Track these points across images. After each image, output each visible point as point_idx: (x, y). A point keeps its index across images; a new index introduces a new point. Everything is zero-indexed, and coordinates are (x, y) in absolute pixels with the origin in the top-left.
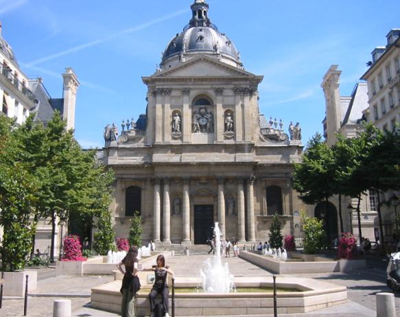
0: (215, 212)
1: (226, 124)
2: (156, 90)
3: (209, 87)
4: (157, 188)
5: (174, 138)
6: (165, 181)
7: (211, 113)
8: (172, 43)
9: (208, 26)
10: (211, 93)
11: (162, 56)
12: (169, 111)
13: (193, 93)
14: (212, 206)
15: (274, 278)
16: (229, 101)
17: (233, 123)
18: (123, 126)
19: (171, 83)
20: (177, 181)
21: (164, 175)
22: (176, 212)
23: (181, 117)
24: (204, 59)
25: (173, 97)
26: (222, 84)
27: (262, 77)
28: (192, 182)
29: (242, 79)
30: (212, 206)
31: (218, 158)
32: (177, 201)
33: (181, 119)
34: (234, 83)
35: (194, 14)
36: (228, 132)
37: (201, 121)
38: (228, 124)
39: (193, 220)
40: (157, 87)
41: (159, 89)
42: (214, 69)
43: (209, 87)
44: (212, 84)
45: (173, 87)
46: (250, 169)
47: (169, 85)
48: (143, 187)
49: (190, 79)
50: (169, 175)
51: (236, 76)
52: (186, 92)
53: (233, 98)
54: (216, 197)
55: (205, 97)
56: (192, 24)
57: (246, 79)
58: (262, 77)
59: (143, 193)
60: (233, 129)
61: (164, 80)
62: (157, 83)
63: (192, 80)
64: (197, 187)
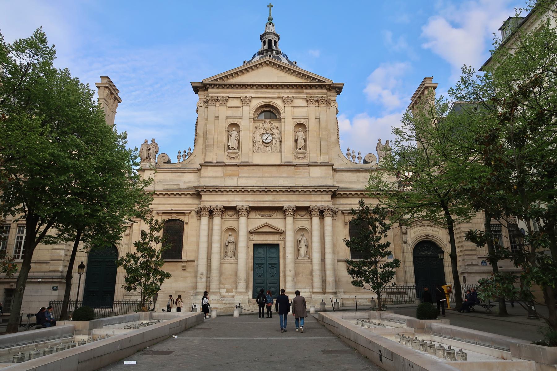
0: (281, 254)
1: (296, 141)
2: (208, 98)
4: (205, 220)
5: (231, 158)
7: (277, 128)
10: (278, 103)
12: (225, 124)
13: (256, 103)
14: (278, 245)
16: (301, 113)
17: (305, 140)
18: (179, 157)
19: (228, 90)
21: (214, 204)
22: (229, 254)
25: (230, 107)
26: (291, 93)
28: (253, 215)
29: (315, 86)
30: (276, 246)
31: (285, 182)
32: (232, 239)
34: (305, 91)
36: (300, 151)
37: (265, 137)
38: (299, 142)
39: (251, 264)
40: (210, 95)
41: (212, 97)
43: (276, 96)
44: (279, 93)
45: (230, 95)
46: (328, 197)
47: (226, 93)
48: (186, 221)
50: (220, 204)
51: (308, 82)
52: (246, 101)
54: (282, 233)
59: (185, 226)
60: (305, 147)
64: (257, 221)
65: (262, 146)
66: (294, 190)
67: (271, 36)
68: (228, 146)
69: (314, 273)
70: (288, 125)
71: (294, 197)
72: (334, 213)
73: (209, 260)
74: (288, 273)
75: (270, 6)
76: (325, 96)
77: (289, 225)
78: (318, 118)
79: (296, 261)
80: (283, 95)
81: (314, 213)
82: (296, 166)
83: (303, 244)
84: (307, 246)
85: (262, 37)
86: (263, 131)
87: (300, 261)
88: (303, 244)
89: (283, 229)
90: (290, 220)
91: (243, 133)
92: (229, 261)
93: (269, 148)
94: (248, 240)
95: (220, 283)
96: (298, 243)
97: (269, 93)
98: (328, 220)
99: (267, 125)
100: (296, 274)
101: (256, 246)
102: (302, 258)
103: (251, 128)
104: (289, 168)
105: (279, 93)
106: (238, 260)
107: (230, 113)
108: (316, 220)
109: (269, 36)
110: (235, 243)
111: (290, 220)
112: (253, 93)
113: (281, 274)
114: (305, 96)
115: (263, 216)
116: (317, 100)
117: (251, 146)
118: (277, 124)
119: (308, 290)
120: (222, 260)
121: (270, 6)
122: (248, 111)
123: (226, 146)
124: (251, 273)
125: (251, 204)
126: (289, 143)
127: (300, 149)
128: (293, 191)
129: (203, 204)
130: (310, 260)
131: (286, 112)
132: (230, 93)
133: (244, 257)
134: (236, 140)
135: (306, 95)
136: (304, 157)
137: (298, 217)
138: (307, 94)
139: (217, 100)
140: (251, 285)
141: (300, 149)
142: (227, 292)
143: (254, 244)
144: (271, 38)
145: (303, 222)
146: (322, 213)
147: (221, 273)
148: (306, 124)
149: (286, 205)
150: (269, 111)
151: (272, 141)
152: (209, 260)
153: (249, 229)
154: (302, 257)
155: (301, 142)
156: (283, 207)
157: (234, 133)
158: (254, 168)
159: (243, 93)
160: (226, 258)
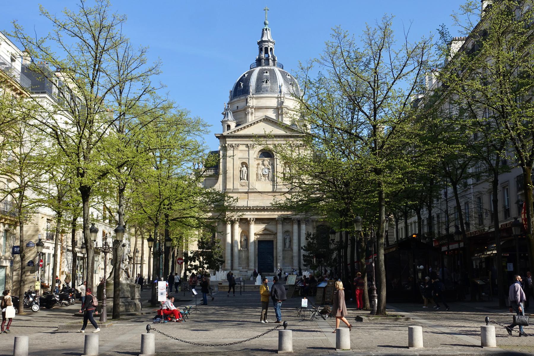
0: (275, 247)
8: (238, 84)
9: (274, 65)
11: (229, 94)
12: (238, 163)
20: (243, 222)
26: (281, 140)
30: (272, 242)
33: (247, 167)
35: (261, 50)
39: (257, 253)
54: (275, 234)
56: (259, 62)
72: (307, 221)
74: (278, 258)
79: (283, 250)
83: (288, 240)
85: (259, 43)
87: (286, 250)
88: (288, 240)
90: (280, 227)
91: (250, 169)
95: (239, 264)
96: (284, 240)
98: (303, 227)
100: (284, 258)
108: (296, 227)
113: (275, 259)
119: (290, 268)
124: (257, 258)
125: (256, 217)
137: (285, 224)
140: (257, 265)
144: (267, 46)
145: (288, 227)
146: (299, 222)
147: (239, 258)
157: (245, 169)
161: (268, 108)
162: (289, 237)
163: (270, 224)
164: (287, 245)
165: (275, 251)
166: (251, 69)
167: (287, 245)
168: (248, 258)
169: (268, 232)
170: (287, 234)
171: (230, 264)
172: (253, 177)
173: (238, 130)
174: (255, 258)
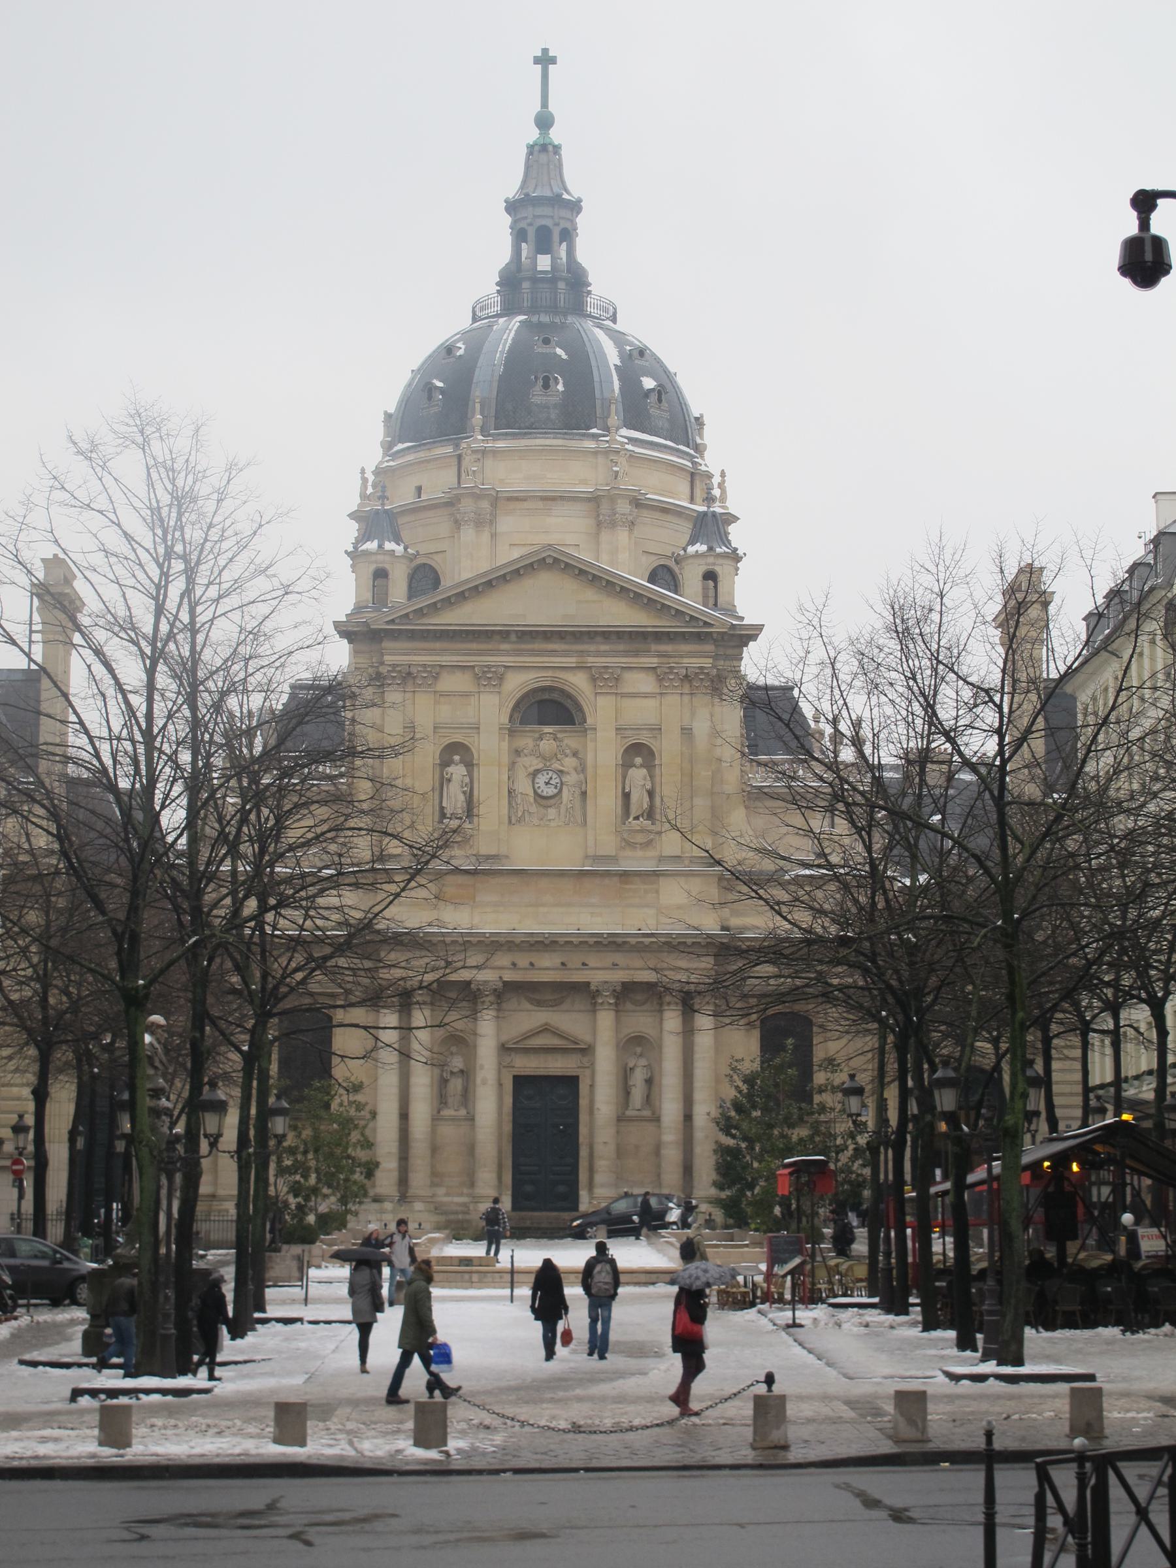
0: (583, 1102)
1: (626, 796)
2: (384, 670)
3: (571, 661)
6: (419, 996)
7: (575, 754)
10: (579, 683)
13: (517, 684)
15: (794, 1318)
16: (641, 712)
17: (651, 794)
19: (438, 645)
22: (450, 1100)
23: (469, 765)
24: (556, 560)
25: (443, 694)
26: (616, 654)
27: (760, 628)
30: (572, 1082)
32: (457, 1063)
34: (654, 647)
35: (519, 236)
37: (541, 779)
38: (634, 798)
39: (508, 1128)
42: (590, 594)
43: (571, 661)
45: (446, 659)
49: (504, 634)
52: (490, 678)
53: (651, 703)
54: (587, 1051)
55: (555, 696)
57: (699, 637)
58: (760, 628)
61: (412, 635)
62: (387, 644)
63: (513, 637)
64: (527, 1018)
65: (533, 809)
66: (619, 940)
67: (547, 211)
68: (442, 808)
69: (663, 1152)
70: (603, 750)
71: (619, 958)
73: (404, 1116)
74: (599, 1149)
75: (545, 60)
76: (707, 663)
77: (604, 1031)
78: (687, 732)
79: (621, 1119)
80: (590, 659)
81: (668, 999)
82: (625, 875)
83: (638, 1077)
84: (649, 1082)
86: (537, 764)
87: (631, 1120)
89: (588, 1038)
90: (605, 1019)
92: (453, 1119)
93: (552, 812)
94: (501, 1067)
95: (434, 1174)
96: (625, 1074)
97: (553, 653)
98: (704, 1022)
99: (547, 745)
100: (620, 1152)
101: (521, 1083)
102: (637, 1113)
103: (505, 759)
104: (607, 881)
105: (582, 653)
106: (477, 1118)
107: (445, 712)
108: (672, 1020)
109: (539, 211)
110: (467, 1074)
111: (605, 1019)
112: (507, 653)
113: (583, 1153)
114: (653, 661)
115: (539, 1003)
116: (686, 676)
117: (505, 811)
118: (571, 741)
120: (436, 1119)
121: (545, 60)
122: (491, 710)
123: (437, 814)
125: (509, 976)
126: (606, 801)
127: (637, 818)
128: (614, 942)
129: (384, 974)
130: (656, 1119)
131: (601, 711)
132: (443, 652)
133: (490, 1107)
134: (464, 793)
135: (655, 660)
136: (648, 844)
137: (629, 1006)
138: (661, 655)
139: (409, 674)
140: (508, 1178)
141: (637, 818)
142: (447, 1194)
143: (515, 1077)
144: (548, 222)
145: (640, 1021)
146: (688, 1003)
147: (434, 1149)
148: (654, 745)
149: (596, 977)
150: (551, 709)
151: (561, 790)
152: (404, 1116)
153: (504, 1038)
154: (637, 1110)
155: (639, 799)
156: (588, 984)
157: (457, 771)
158: (515, 880)
159: (481, 653)
160: (447, 1112)
161: (553, 499)
162: (643, 1062)
163: (565, 1006)
164: (638, 1094)
165: (583, 1117)
166: (475, 319)
167: (638, 1094)
168: (471, 1149)
169: (555, 1042)
170: (635, 1045)
171: (395, 1175)
172: (492, 809)
173: (434, 608)
174: (500, 1152)
